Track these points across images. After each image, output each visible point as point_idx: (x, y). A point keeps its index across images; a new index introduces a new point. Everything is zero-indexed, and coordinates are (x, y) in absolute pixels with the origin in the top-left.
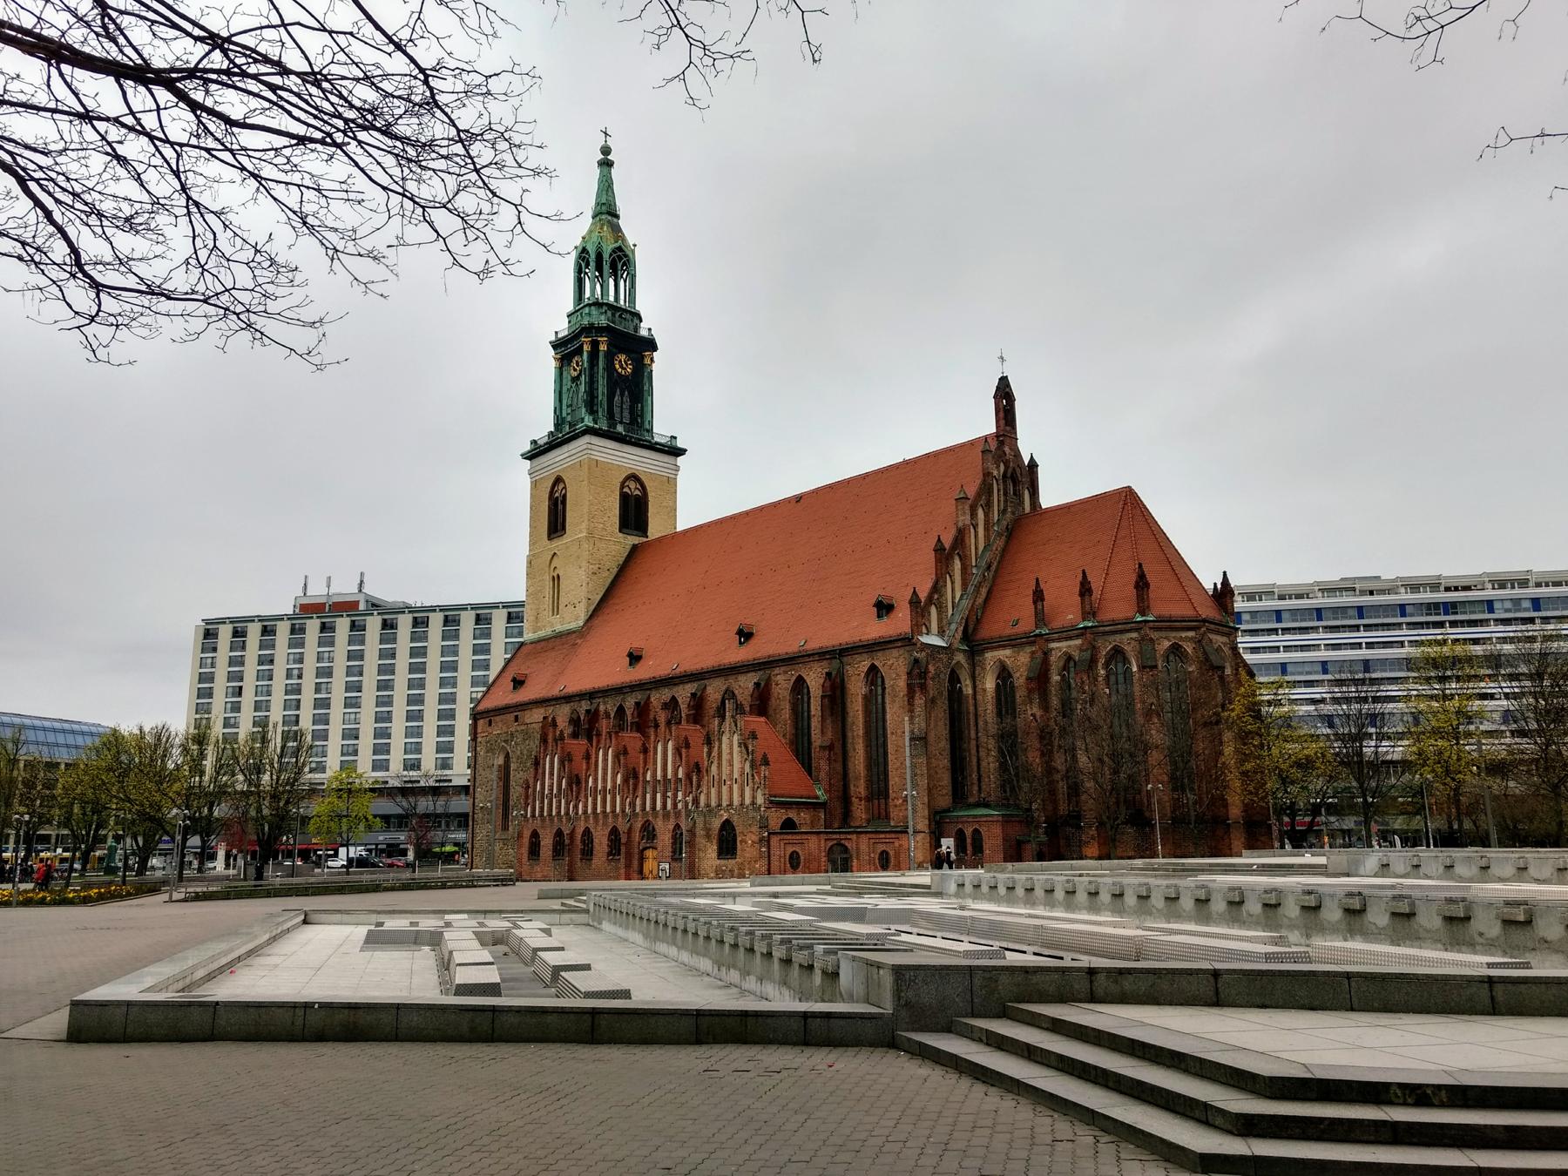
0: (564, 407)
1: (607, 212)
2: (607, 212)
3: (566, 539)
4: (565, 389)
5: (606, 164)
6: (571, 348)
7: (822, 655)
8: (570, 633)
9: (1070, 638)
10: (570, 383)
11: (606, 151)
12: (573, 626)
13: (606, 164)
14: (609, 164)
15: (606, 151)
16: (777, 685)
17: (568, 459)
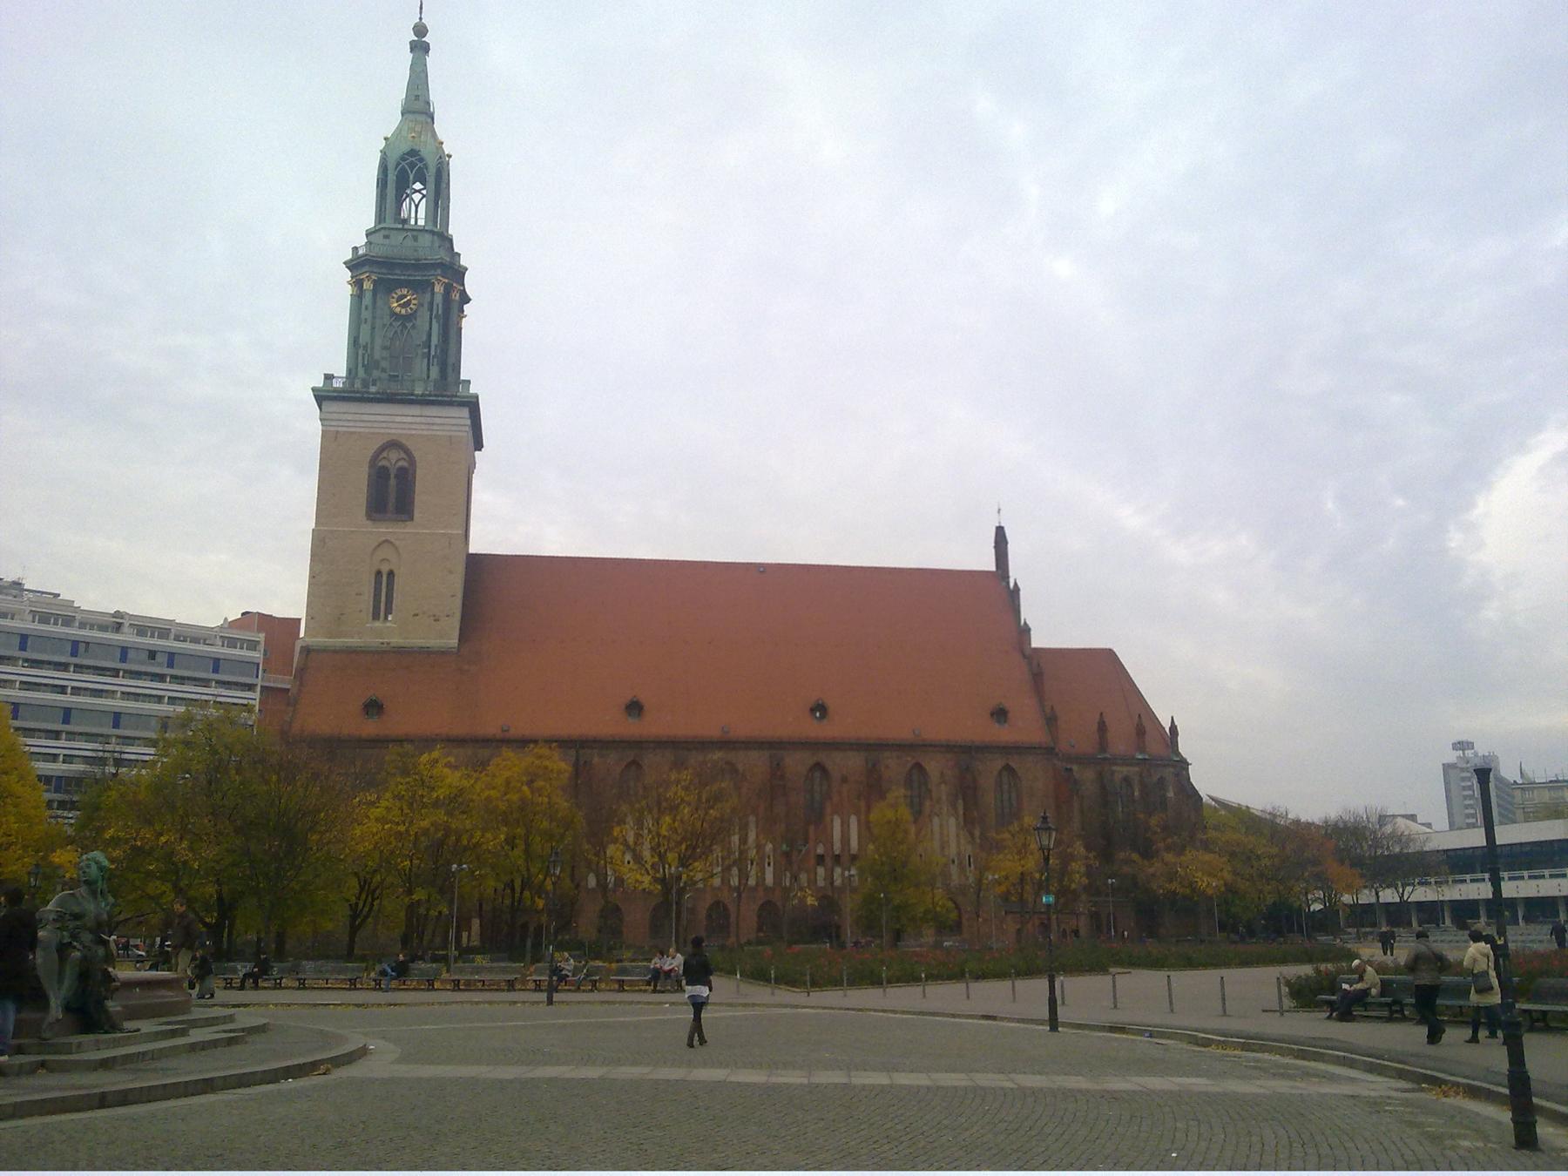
0: (377, 347)
1: (418, 107)
2: (418, 107)
3: (408, 529)
4: (378, 323)
5: (420, 48)
6: (398, 275)
7: (949, 748)
8: (426, 652)
9: (1131, 765)
10: (387, 320)
11: (420, 30)
12: (434, 642)
13: (420, 48)
14: (425, 48)
15: (420, 30)
16: (887, 767)
17: (423, 427)
